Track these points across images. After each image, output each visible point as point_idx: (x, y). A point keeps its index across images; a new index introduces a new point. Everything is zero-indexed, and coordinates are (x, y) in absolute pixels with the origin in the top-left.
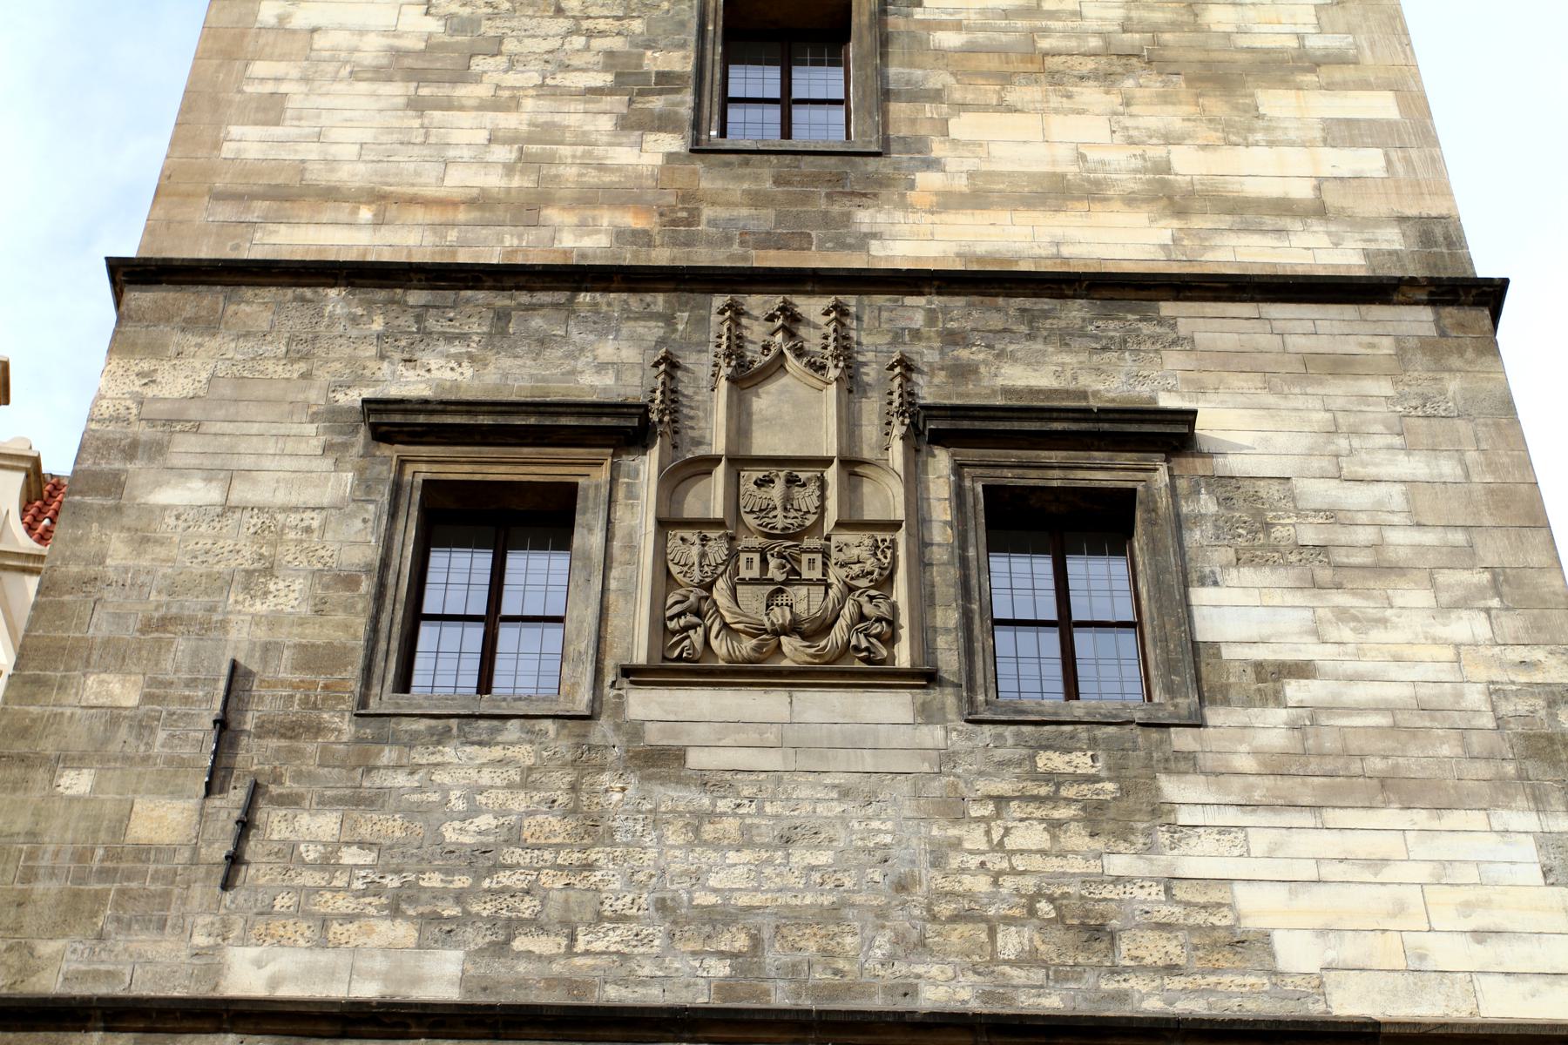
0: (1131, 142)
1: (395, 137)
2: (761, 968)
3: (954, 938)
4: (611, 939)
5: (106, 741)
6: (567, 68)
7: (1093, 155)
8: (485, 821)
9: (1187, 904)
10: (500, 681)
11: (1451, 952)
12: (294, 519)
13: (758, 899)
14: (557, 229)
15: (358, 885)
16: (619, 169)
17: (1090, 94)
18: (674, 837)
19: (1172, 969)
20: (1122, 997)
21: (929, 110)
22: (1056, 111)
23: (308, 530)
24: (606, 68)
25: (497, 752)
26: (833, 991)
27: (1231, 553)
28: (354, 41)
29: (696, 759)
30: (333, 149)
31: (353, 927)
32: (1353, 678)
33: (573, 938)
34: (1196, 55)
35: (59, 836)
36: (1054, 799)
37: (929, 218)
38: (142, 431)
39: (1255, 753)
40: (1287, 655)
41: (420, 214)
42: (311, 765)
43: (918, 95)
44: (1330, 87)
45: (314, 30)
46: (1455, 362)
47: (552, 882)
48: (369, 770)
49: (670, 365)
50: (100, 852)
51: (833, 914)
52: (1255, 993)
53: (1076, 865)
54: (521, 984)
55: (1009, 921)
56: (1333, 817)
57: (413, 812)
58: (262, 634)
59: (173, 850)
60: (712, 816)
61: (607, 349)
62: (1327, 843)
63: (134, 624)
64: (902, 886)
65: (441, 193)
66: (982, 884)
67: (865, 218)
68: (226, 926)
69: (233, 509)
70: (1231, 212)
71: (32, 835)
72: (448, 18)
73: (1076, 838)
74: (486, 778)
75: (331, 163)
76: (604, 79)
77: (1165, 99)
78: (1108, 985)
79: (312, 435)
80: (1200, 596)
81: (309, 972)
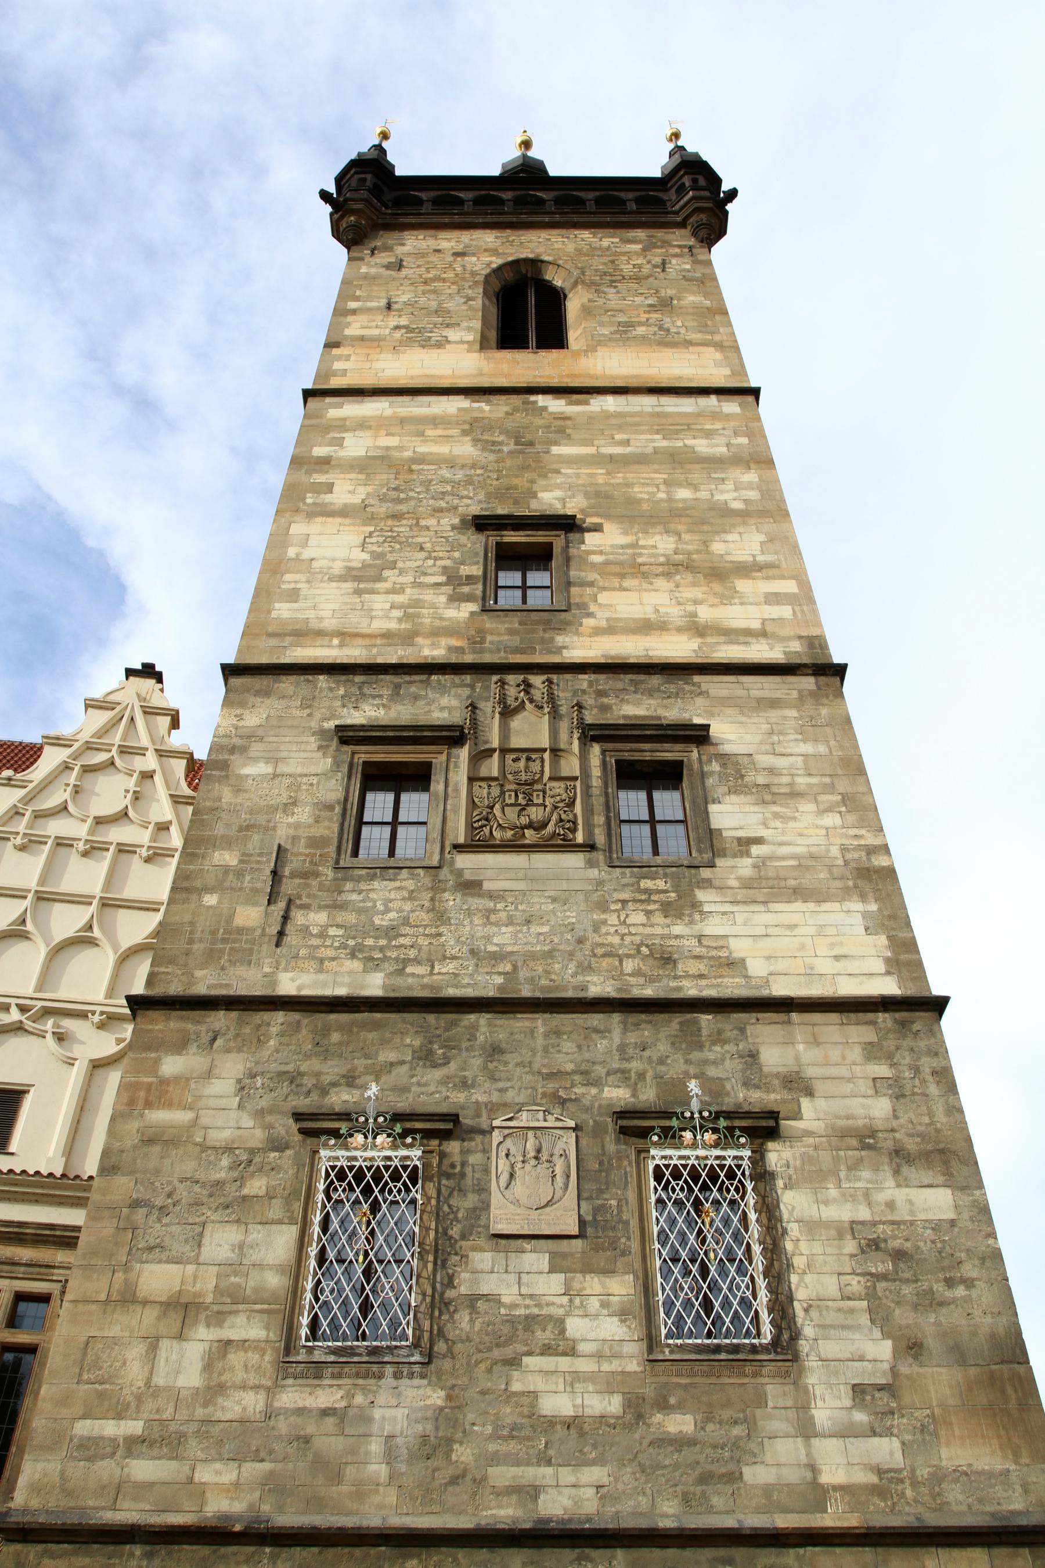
0: (679, 603)
1: (349, 607)
2: (517, 978)
3: (604, 964)
4: (450, 967)
5: (224, 881)
6: (425, 574)
7: (662, 610)
8: (393, 915)
9: (708, 947)
10: (399, 852)
11: (825, 966)
12: (305, 780)
13: (516, 948)
14: (421, 647)
15: (336, 944)
16: (449, 619)
17: (661, 583)
18: (478, 920)
19: (701, 976)
20: (679, 989)
21: (588, 590)
22: (646, 590)
23: (311, 785)
24: (443, 574)
25: (397, 884)
26: (550, 989)
27: (726, 789)
28: (330, 564)
29: (487, 886)
30: (321, 613)
31: (334, 963)
33: (433, 967)
34: (707, 565)
36: (648, 901)
37: (589, 639)
38: (237, 741)
39: (737, 878)
40: (752, 834)
41: (360, 641)
42: (314, 891)
43: (583, 584)
44: (767, 578)
45: (312, 560)
46: (825, 701)
47: (423, 942)
48: (340, 892)
49: (473, 707)
50: (221, 931)
51: (549, 955)
52: (738, 986)
53: (658, 930)
54: (410, 988)
55: (628, 956)
56: (773, 906)
57: (360, 911)
58: (291, 832)
59: (254, 930)
60: (494, 911)
61: (445, 701)
63: (235, 828)
64: (580, 941)
65: (369, 631)
66: (616, 940)
67: (560, 640)
68: (278, 963)
69: (278, 776)
70: (724, 635)
71: (192, 923)
72: (372, 553)
73: (658, 918)
74: (393, 895)
75: (320, 619)
77: (694, 584)
78: (673, 984)
79: (313, 742)
80: (713, 808)
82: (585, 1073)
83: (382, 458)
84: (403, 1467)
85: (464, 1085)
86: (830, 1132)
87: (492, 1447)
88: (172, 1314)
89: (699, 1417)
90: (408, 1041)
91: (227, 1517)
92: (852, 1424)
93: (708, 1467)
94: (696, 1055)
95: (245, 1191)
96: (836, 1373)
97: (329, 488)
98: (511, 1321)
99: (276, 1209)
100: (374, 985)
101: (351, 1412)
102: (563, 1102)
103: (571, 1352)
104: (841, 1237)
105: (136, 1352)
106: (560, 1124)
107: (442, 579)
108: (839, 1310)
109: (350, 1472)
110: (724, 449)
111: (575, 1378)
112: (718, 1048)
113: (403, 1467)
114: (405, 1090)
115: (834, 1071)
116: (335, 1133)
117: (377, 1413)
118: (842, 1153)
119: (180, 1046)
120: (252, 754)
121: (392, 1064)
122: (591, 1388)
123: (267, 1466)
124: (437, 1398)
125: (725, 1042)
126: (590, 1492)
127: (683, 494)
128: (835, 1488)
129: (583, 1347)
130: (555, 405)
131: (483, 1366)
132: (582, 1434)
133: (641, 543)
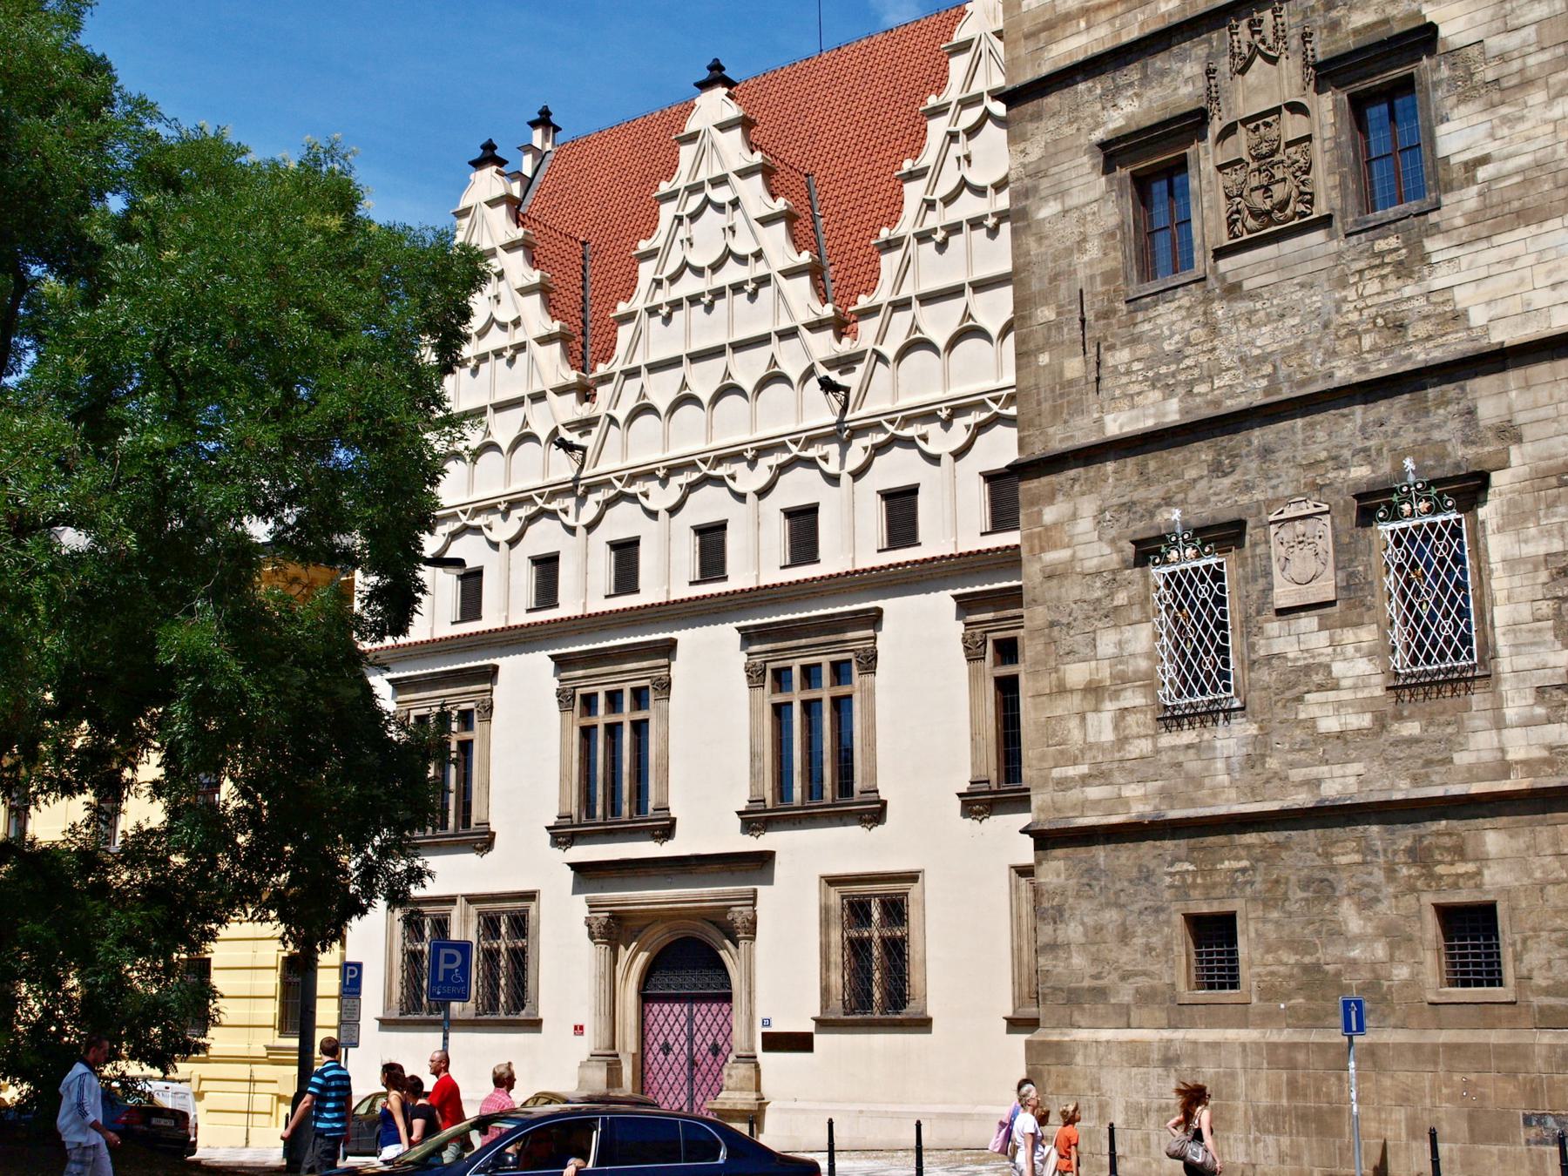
3: (1346, 346)
4: (1226, 379)
5: (1049, 338)
8: (1177, 337)
11: (1541, 298)
12: (1087, 210)
13: (1275, 347)
15: (1140, 378)
18: (1242, 326)
19: (1429, 338)
20: (1409, 357)
23: (1094, 213)
25: (1176, 304)
26: (1302, 384)
29: (1247, 285)
32: (1507, 158)
33: (1212, 383)
35: (1045, 381)
36: (1383, 265)
38: (1028, 182)
40: (1477, 153)
41: (1104, 15)
47: (1203, 359)
49: (1210, 73)
51: (1301, 347)
53: (1391, 296)
55: (1366, 331)
56: (1497, 240)
57: (1154, 340)
58: (1088, 271)
60: (1256, 311)
62: (1492, 255)
63: (1046, 281)
64: (1326, 326)
66: (1354, 317)
68: (1102, 407)
71: (1037, 386)
73: (1392, 283)
74: (1174, 317)
80: (1441, 130)
81: (1131, 420)
82: (1335, 458)
84: (1237, 776)
85: (1248, 488)
86: (1534, 476)
87: (1290, 757)
88: (1089, 696)
89: (1424, 723)
90: (1203, 457)
91: (1142, 816)
92: (1533, 716)
93: (1430, 756)
94: (1423, 423)
95: (1115, 603)
96: (1524, 680)
98: (1300, 669)
99: (1136, 614)
100: (1172, 413)
101: (1203, 744)
102: (1320, 488)
103: (1336, 687)
104: (1536, 569)
105: (1073, 723)
106: (1317, 510)
108: (1530, 631)
109: (1207, 781)
111: (1340, 705)
112: (1441, 411)
113: (1237, 776)
114: (1203, 502)
115: (1542, 413)
116: (1157, 552)
117: (1218, 743)
118: (1543, 493)
119: (1051, 499)
120: (1043, 194)
121: (1195, 480)
122: (1350, 711)
123: (1160, 783)
124: (1253, 729)
125: (1448, 403)
126: (1352, 780)
128: (1517, 763)
129: (1345, 683)
131: (1280, 704)
132: (1346, 742)
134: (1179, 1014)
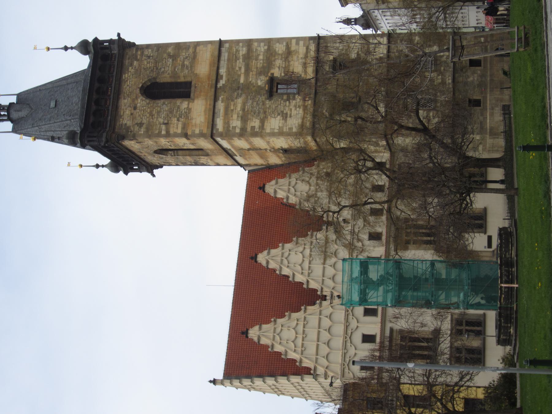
0: (298, 60)
6: (286, 105)
17: (292, 63)
44: (291, 44)
72: (278, 115)
76: (288, 102)
77: (292, 57)
83: (242, 117)
97: (253, 128)
107: (288, 102)
110: (244, 49)
127: (261, 57)
130: (222, 83)
133: (278, 66)
134: (485, 109)
